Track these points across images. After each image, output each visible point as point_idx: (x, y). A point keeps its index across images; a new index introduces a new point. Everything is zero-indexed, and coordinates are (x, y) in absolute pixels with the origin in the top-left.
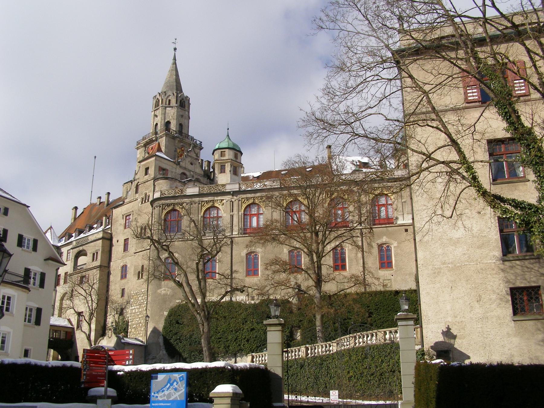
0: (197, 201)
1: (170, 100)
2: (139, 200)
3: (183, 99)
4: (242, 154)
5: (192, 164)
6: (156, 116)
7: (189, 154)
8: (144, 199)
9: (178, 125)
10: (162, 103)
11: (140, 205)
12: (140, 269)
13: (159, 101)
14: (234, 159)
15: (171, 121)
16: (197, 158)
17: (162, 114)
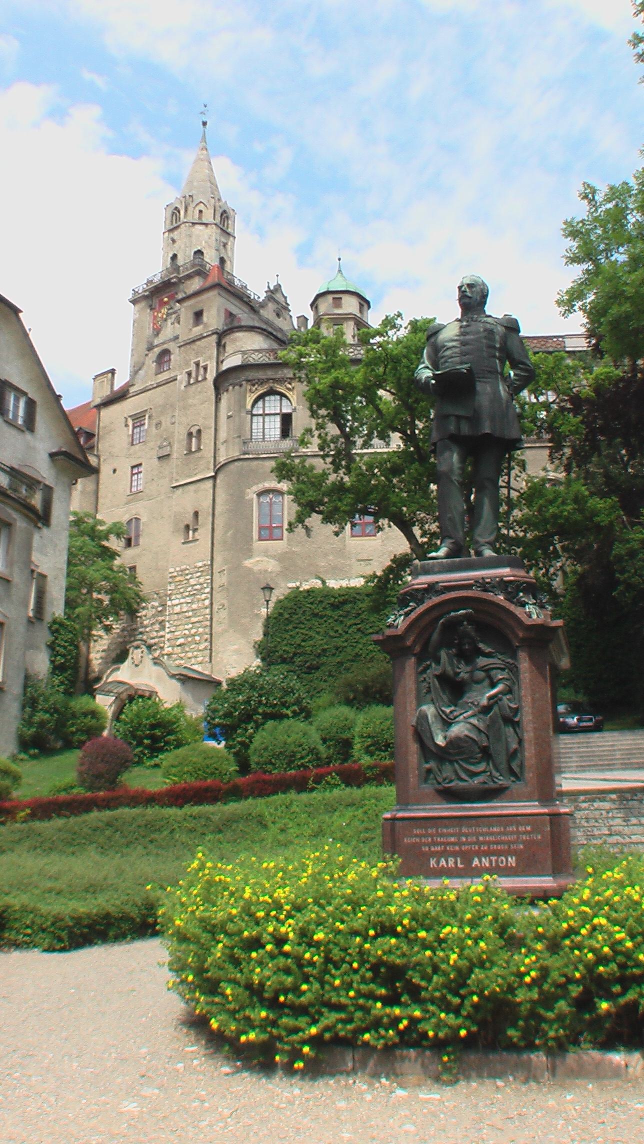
2: (182, 377)
4: (369, 307)
5: (278, 315)
6: (174, 241)
11: (182, 387)
12: (189, 519)
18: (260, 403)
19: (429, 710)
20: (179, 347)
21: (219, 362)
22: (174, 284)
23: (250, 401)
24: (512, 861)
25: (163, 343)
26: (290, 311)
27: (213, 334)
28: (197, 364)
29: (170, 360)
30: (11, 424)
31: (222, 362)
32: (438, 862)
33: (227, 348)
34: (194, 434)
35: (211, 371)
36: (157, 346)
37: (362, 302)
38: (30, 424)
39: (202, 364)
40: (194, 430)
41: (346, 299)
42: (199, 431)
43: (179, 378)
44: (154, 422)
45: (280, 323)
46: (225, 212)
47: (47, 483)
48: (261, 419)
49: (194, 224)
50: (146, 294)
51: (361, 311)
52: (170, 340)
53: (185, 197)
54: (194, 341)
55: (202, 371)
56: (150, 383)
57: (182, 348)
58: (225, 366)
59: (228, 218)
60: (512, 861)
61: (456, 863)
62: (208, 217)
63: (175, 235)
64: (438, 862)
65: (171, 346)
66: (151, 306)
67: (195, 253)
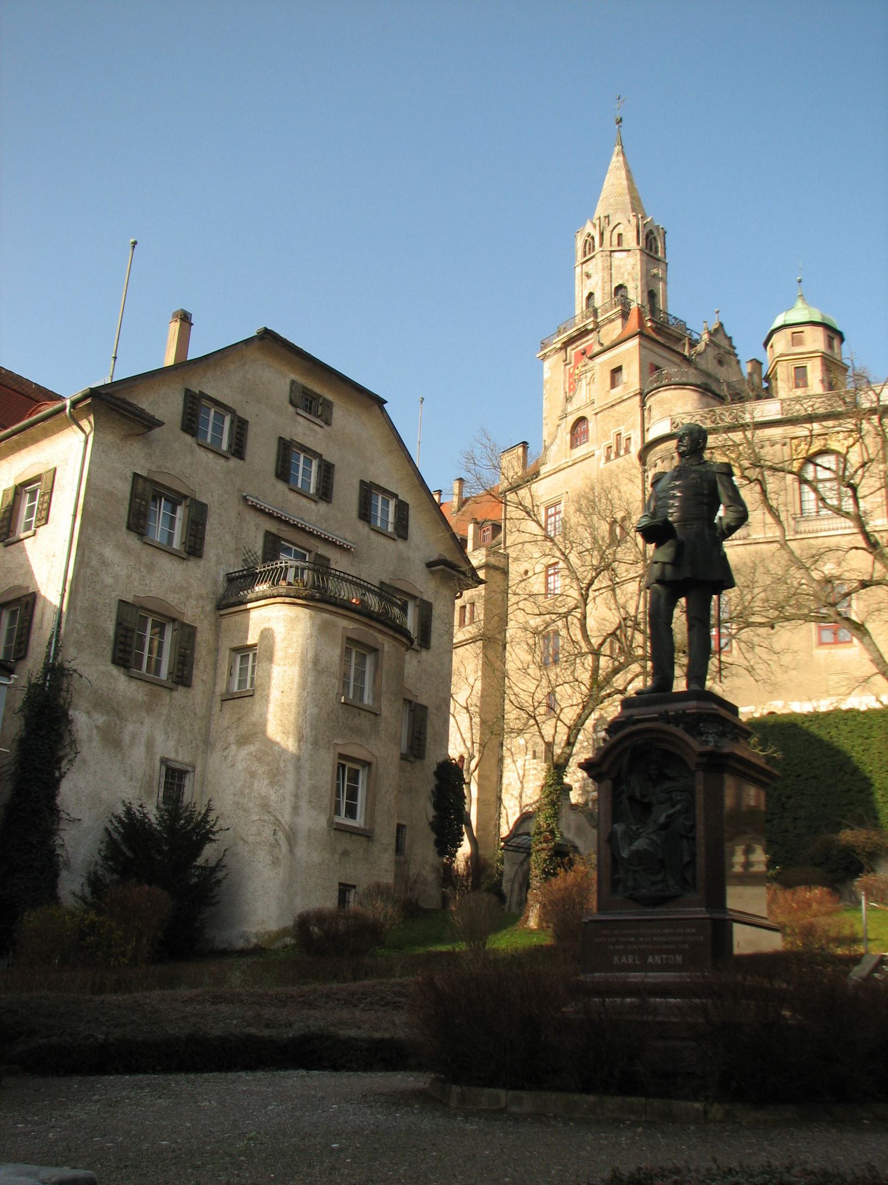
0: (777, 438)
1: (620, 235)
2: (601, 452)
4: (842, 340)
5: (720, 363)
6: (588, 276)
7: (713, 339)
8: (614, 449)
9: (646, 294)
10: (601, 245)
13: (593, 238)
14: (828, 352)
15: (630, 286)
16: (732, 350)
17: (603, 269)
20: (596, 414)
21: (644, 431)
24: (679, 959)
25: (578, 409)
26: (736, 355)
27: (635, 395)
29: (588, 429)
30: (381, 533)
31: (648, 430)
32: (620, 959)
33: (653, 412)
35: (636, 443)
36: (571, 413)
37: (832, 335)
38: (402, 530)
43: (597, 453)
45: (722, 373)
46: (651, 232)
47: (425, 598)
52: (586, 406)
53: (599, 218)
54: (613, 406)
56: (564, 461)
57: (599, 415)
58: (650, 437)
60: (679, 959)
61: (634, 961)
62: (630, 240)
64: (620, 959)
65: (587, 413)
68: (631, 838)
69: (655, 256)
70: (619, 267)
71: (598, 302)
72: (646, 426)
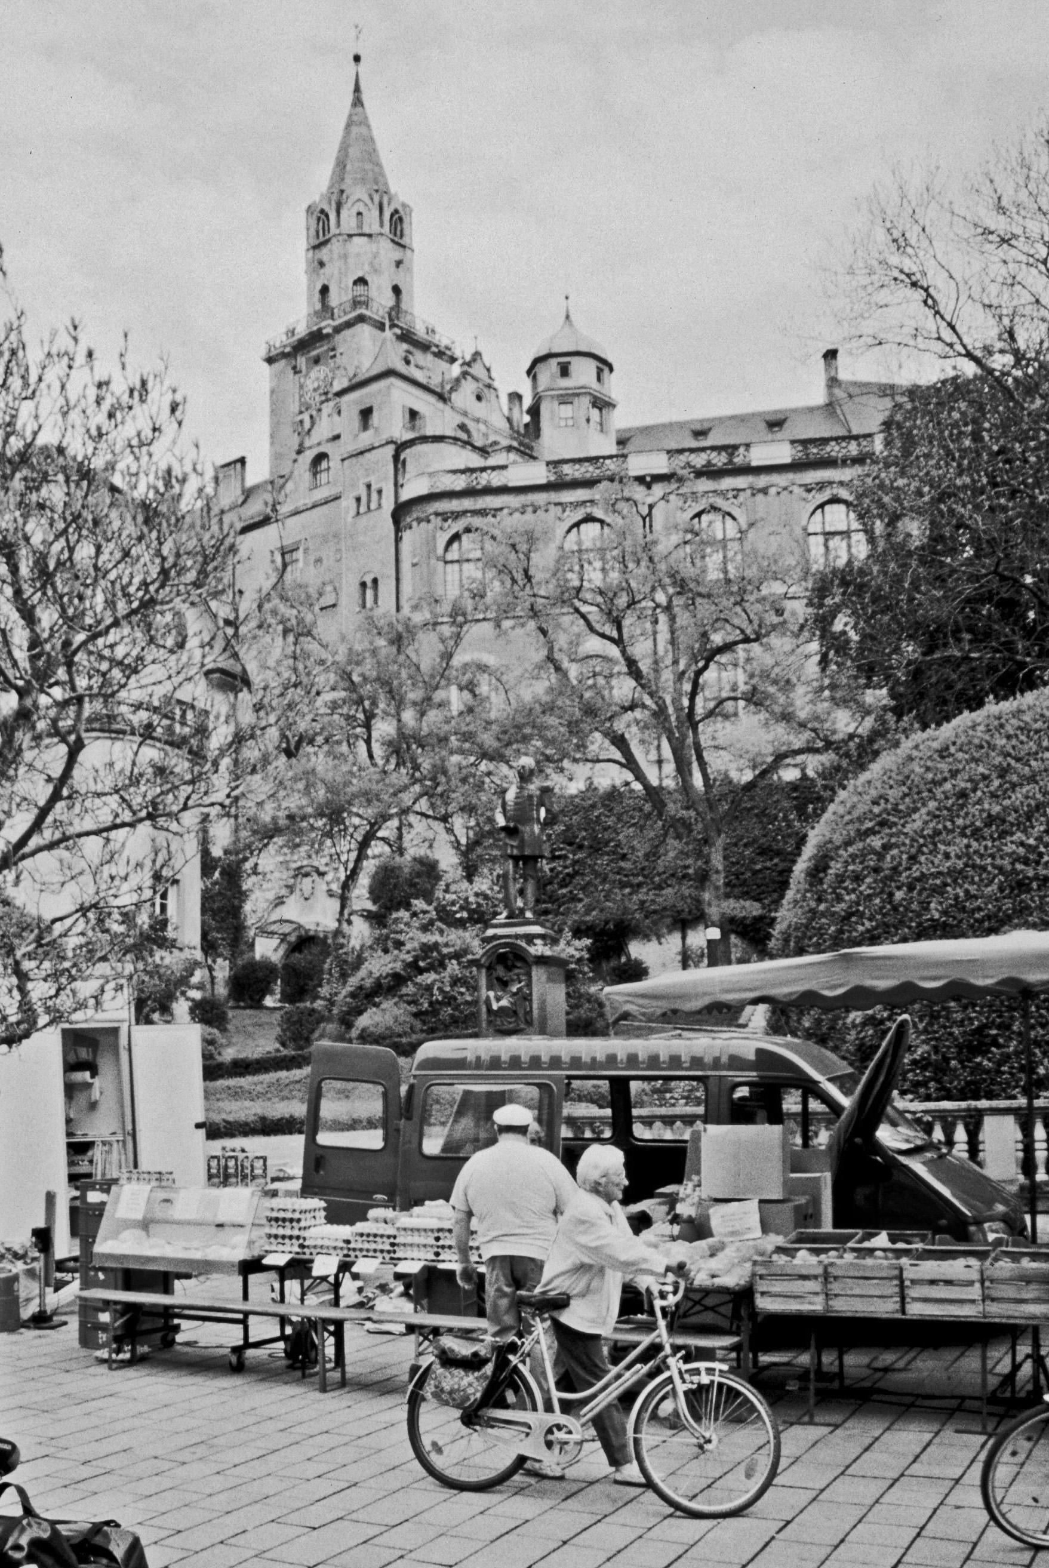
2: (347, 503)
3: (396, 211)
5: (479, 398)
6: (322, 264)
11: (350, 519)
13: (327, 216)
18: (456, 545)
19: (491, 994)
21: (397, 486)
22: (328, 336)
23: (443, 538)
25: (319, 444)
27: (388, 443)
28: (369, 486)
34: (369, 584)
36: (310, 448)
39: (374, 487)
40: (368, 580)
41: (576, 364)
42: (375, 581)
44: (312, 558)
48: (456, 566)
49: (350, 236)
50: (288, 350)
51: (599, 379)
54: (362, 453)
55: (374, 496)
57: (346, 462)
58: (406, 495)
59: (401, 219)
63: (324, 254)
66: (294, 368)
67: (355, 283)
68: (498, 999)
69: (402, 242)
70: (358, 255)
71: (335, 299)
72: (401, 481)
